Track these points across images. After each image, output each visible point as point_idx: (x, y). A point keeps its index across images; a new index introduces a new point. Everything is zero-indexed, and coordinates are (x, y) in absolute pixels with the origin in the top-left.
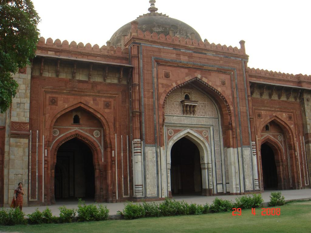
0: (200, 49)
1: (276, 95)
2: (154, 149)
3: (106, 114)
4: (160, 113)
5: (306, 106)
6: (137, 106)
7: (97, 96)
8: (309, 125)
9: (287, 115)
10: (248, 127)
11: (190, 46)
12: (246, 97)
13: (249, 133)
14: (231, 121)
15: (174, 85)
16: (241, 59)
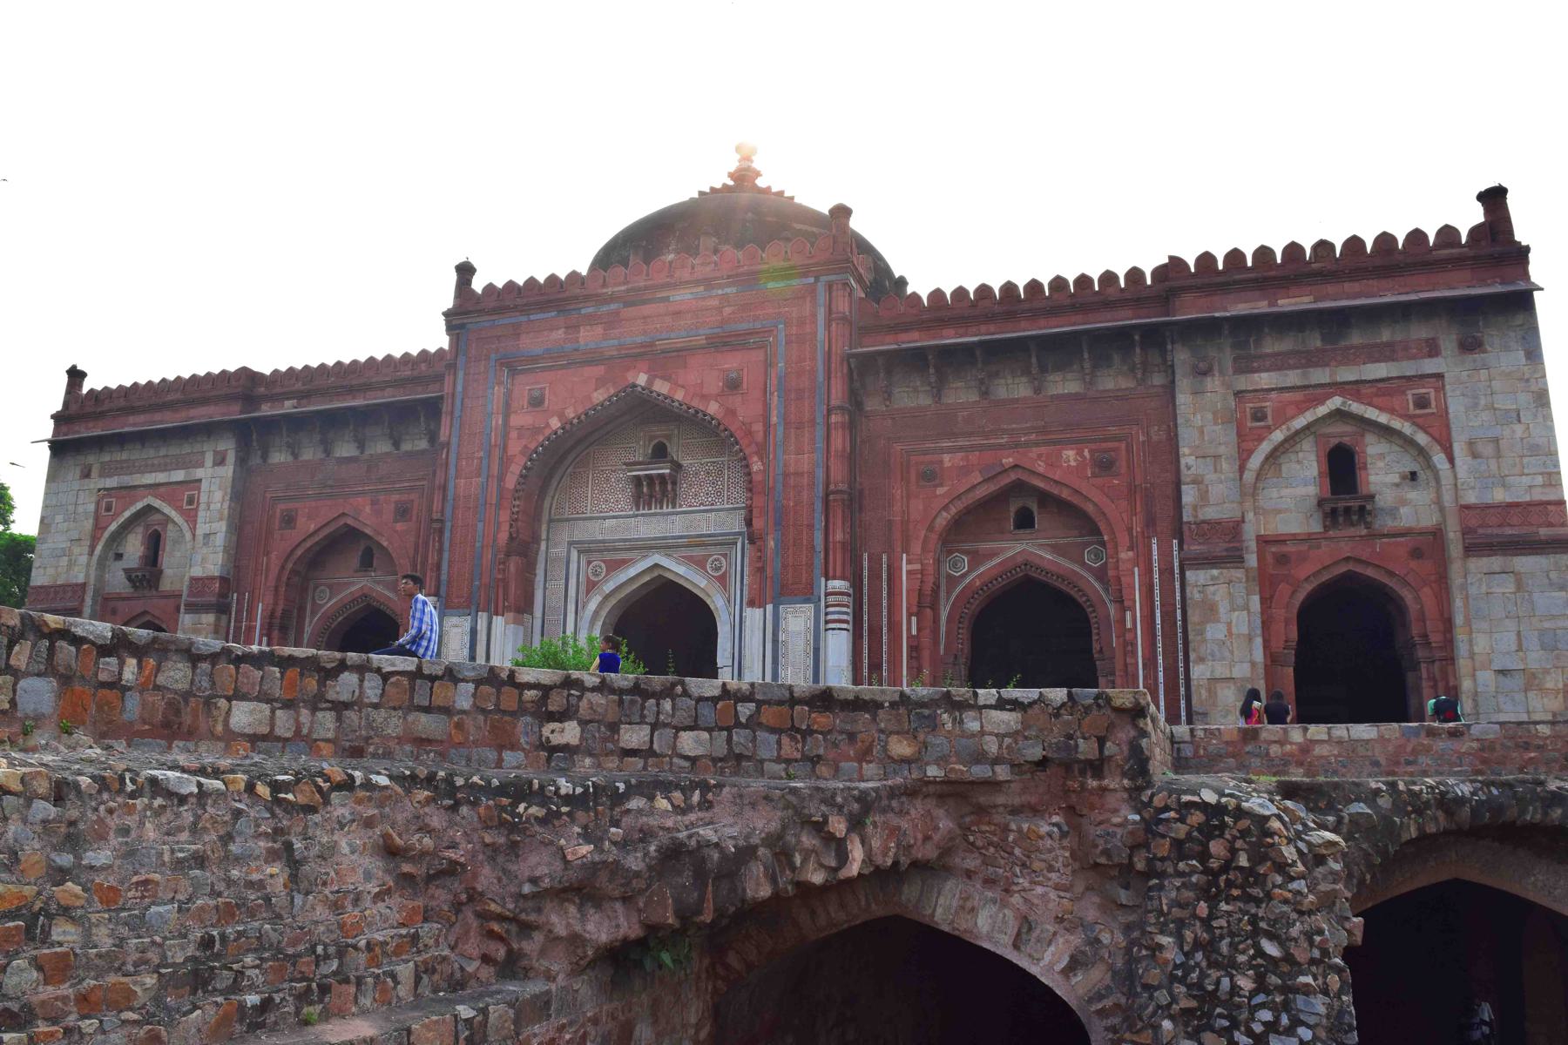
0: (646, 288)
1: (1024, 379)
2: (466, 623)
3: (394, 536)
4: (505, 516)
5: (1183, 399)
6: (436, 506)
7: (378, 491)
8: (1194, 482)
9: (1086, 453)
10: (811, 527)
11: (609, 290)
12: (820, 419)
13: (813, 547)
14: (751, 511)
15: (555, 423)
16: (812, 280)
